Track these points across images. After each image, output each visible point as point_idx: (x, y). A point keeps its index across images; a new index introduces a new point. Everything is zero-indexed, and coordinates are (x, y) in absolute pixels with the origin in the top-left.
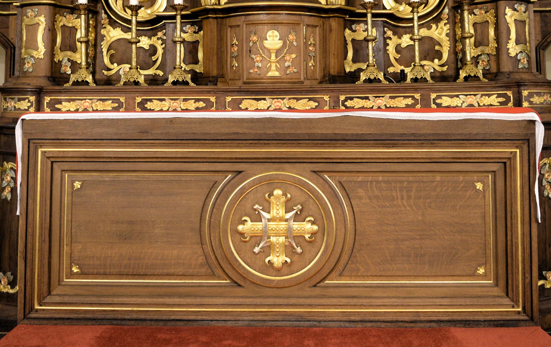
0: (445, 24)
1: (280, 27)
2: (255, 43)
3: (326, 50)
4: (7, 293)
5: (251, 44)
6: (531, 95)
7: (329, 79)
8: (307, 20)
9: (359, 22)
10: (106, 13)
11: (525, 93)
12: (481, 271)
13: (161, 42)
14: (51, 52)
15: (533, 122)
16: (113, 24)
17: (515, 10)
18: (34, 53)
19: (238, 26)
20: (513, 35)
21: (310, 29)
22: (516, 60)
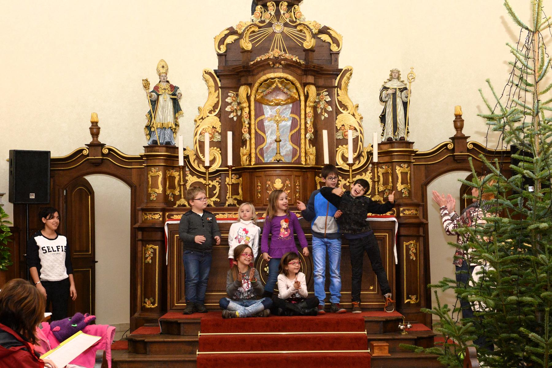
0: (370, 173)
1: (282, 177)
4: (151, 308)
5: (267, 186)
6: (404, 210)
8: (295, 173)
10: (188, 168)
11: (401, 209)
12: (372, 288)
14: (164, 190)
16: (192, 174)
17: (401, 167)
18: (157, 190)
21: (296, 178)
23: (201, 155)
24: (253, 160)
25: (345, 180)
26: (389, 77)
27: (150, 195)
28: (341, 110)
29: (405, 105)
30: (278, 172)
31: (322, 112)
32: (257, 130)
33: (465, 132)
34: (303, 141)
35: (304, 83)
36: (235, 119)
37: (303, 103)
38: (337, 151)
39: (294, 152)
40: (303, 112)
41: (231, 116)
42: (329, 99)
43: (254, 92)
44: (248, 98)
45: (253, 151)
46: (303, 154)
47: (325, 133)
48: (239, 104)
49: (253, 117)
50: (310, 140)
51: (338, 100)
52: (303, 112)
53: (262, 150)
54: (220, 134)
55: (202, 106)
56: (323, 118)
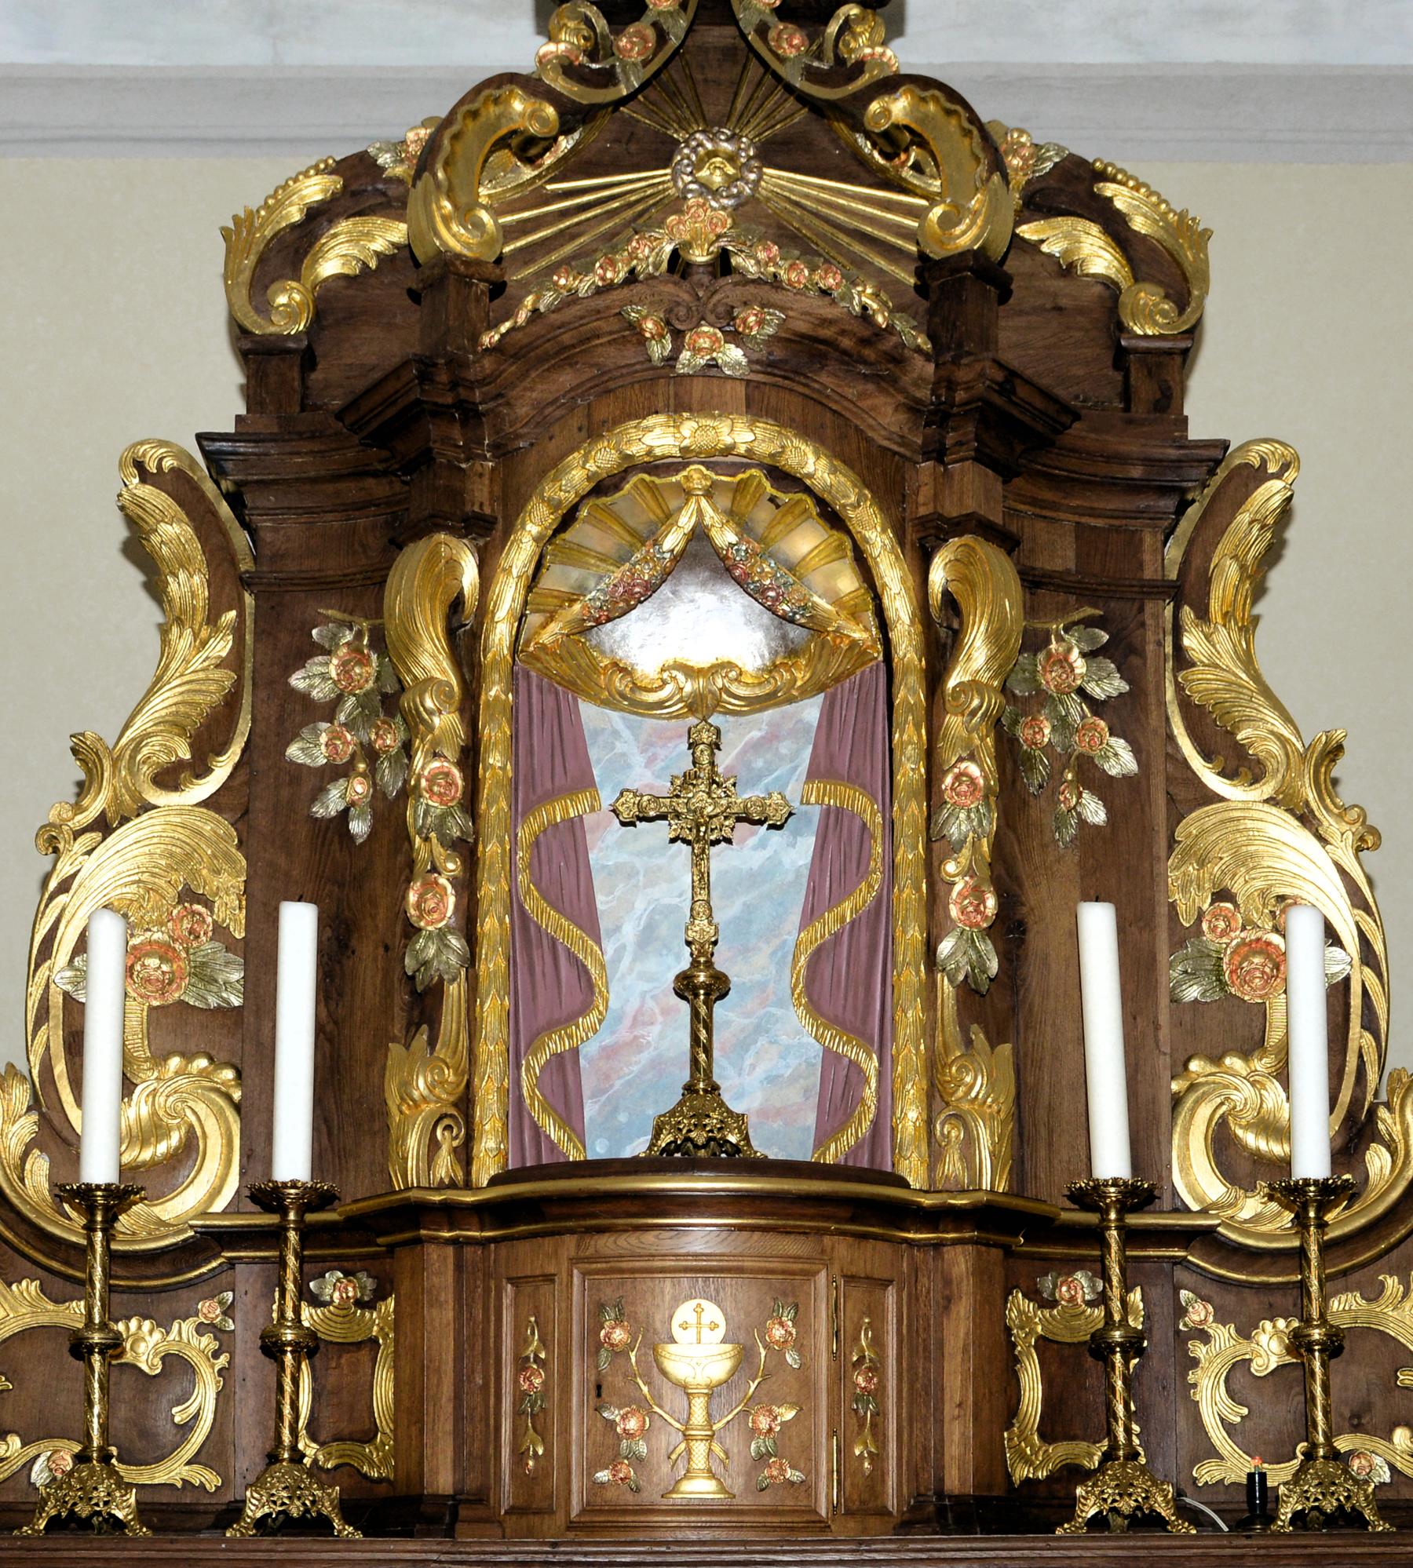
1: (730, 1285)
2: (619, 1353)
3: (926, 1388)
7: (941, 1511)
9: (1072, 1264)
13: (215, 1345)
19: (549, 1278)
21: (857, 1293)
24: (488, 1144)
25: (1245, 1333)
30: (702, 1236)
31: (1055, 777)
32: (533, 904)
35: (923, 522)
37: (910, 693)
38: (1177, 1101)
41: (332, 802)
42: (1110, 686)
43: (508, 595)
47: (1098, 925)
49: (495, 806)
50: (969, 993)
51: (1187, 707)
52: (910, 769)
53: (565, 1066)
55: (103, 729)
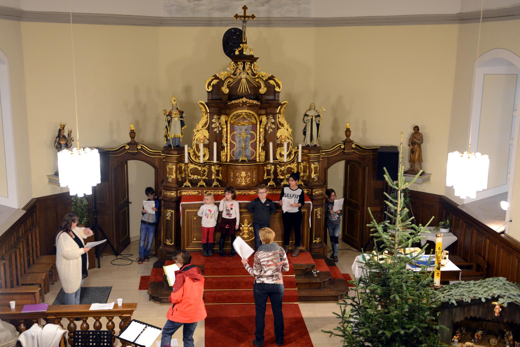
14: (176, 176)
15: (310, 204)
18: (172, 176)
20: (313, 172)
22: (314, 179)
23: (197, 153)
26: (309, 108)
27: (168, 178)
28: (280, 126)
29: (318, 125)
33: (351, 138)
34: (258, 148)
36: (218, 132)
37: (258, 126)
39: (253, 154)
40: (258, 131)
41: (215, 130)
42: (273, 121)
43: (229, 119)
44: (226, 122)
45: (229, 154)
46: (258, 156)
48: (220, 124)
50: (262, 147)
54: (208, 140)
56: (269, 132)
